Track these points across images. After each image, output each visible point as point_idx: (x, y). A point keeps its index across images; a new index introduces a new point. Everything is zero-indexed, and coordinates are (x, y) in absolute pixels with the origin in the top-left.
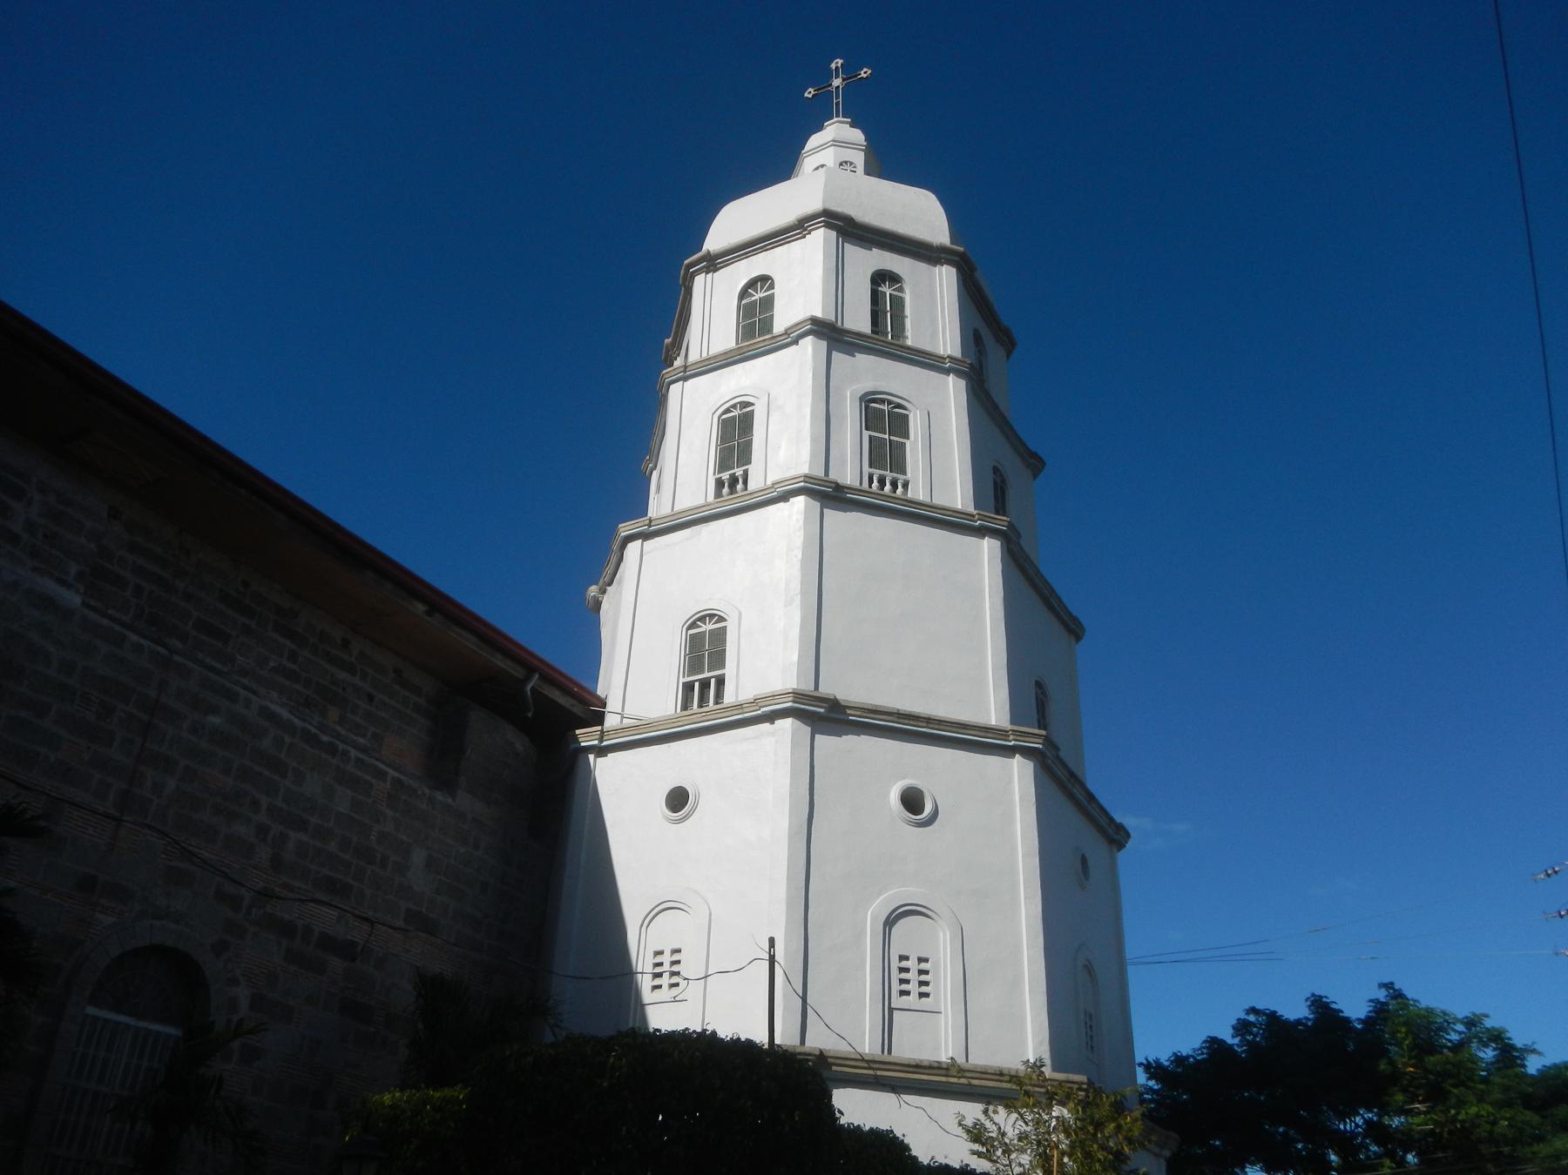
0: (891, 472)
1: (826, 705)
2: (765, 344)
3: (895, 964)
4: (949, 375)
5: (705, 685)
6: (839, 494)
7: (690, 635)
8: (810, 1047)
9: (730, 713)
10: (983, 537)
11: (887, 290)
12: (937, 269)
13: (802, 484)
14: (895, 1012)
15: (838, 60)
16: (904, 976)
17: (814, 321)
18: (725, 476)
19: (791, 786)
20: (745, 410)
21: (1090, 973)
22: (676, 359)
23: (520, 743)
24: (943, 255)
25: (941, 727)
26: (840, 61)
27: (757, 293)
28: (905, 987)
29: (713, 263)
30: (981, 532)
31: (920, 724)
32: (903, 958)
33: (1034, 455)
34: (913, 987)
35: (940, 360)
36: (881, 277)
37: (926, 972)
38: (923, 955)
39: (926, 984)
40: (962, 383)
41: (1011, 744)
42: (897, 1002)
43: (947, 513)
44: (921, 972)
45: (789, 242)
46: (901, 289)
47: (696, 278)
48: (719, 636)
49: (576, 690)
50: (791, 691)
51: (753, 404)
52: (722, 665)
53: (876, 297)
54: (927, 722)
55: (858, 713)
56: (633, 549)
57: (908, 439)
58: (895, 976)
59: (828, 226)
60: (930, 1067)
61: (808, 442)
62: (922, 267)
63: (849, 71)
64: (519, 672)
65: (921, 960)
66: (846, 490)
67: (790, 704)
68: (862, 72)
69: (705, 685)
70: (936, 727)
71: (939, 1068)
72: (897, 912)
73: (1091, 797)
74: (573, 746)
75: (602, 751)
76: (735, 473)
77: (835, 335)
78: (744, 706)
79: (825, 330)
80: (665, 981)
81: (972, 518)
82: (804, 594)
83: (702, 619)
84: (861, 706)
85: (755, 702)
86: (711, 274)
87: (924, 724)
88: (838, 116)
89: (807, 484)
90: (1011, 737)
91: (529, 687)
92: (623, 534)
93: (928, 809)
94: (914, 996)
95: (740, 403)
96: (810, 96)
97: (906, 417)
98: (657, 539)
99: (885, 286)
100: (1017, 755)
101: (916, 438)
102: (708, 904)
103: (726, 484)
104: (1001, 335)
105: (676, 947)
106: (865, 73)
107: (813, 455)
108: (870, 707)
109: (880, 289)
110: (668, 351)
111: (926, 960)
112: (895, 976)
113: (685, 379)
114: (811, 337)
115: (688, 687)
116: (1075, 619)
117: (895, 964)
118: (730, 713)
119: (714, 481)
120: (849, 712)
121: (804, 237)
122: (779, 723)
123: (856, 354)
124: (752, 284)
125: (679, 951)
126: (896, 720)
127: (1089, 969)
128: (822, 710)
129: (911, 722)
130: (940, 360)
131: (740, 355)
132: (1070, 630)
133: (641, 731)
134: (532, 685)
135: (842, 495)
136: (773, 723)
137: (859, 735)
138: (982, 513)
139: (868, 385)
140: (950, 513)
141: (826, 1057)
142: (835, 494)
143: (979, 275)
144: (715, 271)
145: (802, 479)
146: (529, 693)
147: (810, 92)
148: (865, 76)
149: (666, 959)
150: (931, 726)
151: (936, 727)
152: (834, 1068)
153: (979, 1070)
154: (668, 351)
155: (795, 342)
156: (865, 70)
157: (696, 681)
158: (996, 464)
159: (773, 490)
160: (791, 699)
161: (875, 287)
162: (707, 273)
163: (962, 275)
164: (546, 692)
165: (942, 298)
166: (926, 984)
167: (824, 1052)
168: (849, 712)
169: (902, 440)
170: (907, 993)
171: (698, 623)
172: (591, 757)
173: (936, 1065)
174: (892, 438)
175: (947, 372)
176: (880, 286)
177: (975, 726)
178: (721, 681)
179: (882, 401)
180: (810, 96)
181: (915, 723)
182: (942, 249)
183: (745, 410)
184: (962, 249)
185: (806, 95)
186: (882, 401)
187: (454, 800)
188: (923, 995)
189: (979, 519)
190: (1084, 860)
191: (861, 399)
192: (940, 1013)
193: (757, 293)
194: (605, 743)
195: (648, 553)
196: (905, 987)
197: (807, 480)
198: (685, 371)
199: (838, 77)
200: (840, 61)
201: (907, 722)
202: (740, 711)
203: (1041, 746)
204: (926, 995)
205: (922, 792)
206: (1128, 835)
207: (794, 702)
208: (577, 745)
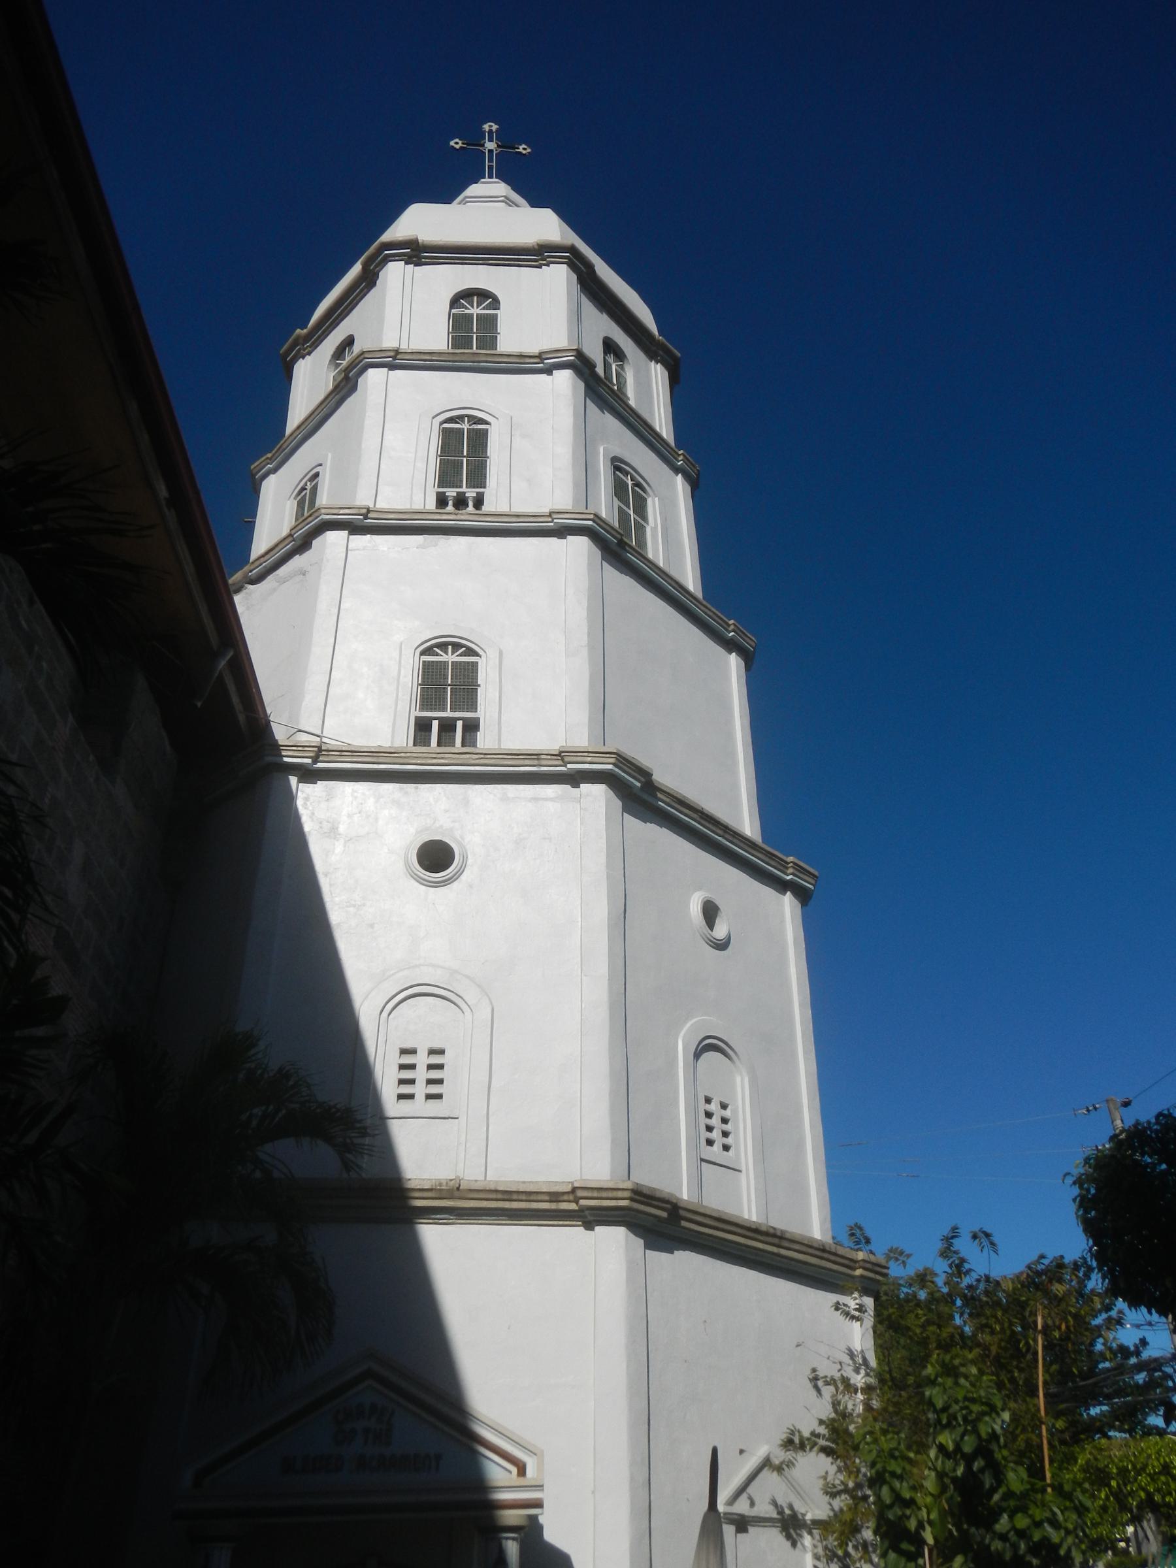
1: (643, 780)
5: (447, 727)
7: (424, 662)
8: (669, 1193)
9: (521, 762)
13: (590, 523)
18: (451, 492)
20: (475, 426)
22: (303, 358)
24: (661, 352)
25: (735, 841)
26: (495, 127)
27: (477, 308)
34: (716, 1135)
41: (788, 878)
47: (390, 264)
49: (254, 690)
51: (487, 423)
54: (725, 832)
55: (668, 800)
57: (648, 524)
59: (572, 265)
60: (767, 1234)
63: (507, 141)
67: (610, 767)
68: (521, 147)
69: (447, 727)
70: (731, 839)
71: (774, 1236)
72: (701, 1046)
76: (445, 493)
78: (543, 757)
79: (586, 371)
81: (726, 626)
82: (591, 647)
83: (443, 646)
84: (671, 792)
85: (561, 755)
88: (491, 177)
89: (595, 525)
90: (790, 870)
93: (720, 931)
94: (717, 1147)
95: (468, 416)
96: (457, 147)
100: (789, 893)
103: (451, 503)
105: (437, 1045)
106: (524, 149)
107: (576, 501)
108: (678, 796)
110: (295, 343)
113: (392, 367)
115: (422, 727)
118: (521, 762)
119: (435, 494)
120: (659, 795)
121: (540, 267)
122: (585, 787)
125: (441, 1052)
126: (698, 819)
128: (639, 785)
133: (381, 760)
137: (661, 827)
138: (737, 624)
139: (618, 452)
144: (417, 265)
145: (592, 517)
147: (457, 143)
149: (422, 1059)
150: (727, 836)
151: (731, 839)
152: (684, 1223)
153: (806, 1242)
154: (295, 343)
155: (548, 371)
157: (435, 718)
159: (550, 520)
160: (612, 760)
162: (407, 263)
168: (659, 795)
172: (293, 780)
173: (772, 1231)
178: (472, 727)
179: (626, 473)
181: (714, 828)
183: (475, 426)
184: (679, 355)
185: (452, 143)
193: (473, 307)
194: (320, 765)
195: (354, 550)
198: (394, 358)
199: (492, 141)
200: (495, 127)
201: (707, 824)
202: (536, 762)
208: (276, 759)
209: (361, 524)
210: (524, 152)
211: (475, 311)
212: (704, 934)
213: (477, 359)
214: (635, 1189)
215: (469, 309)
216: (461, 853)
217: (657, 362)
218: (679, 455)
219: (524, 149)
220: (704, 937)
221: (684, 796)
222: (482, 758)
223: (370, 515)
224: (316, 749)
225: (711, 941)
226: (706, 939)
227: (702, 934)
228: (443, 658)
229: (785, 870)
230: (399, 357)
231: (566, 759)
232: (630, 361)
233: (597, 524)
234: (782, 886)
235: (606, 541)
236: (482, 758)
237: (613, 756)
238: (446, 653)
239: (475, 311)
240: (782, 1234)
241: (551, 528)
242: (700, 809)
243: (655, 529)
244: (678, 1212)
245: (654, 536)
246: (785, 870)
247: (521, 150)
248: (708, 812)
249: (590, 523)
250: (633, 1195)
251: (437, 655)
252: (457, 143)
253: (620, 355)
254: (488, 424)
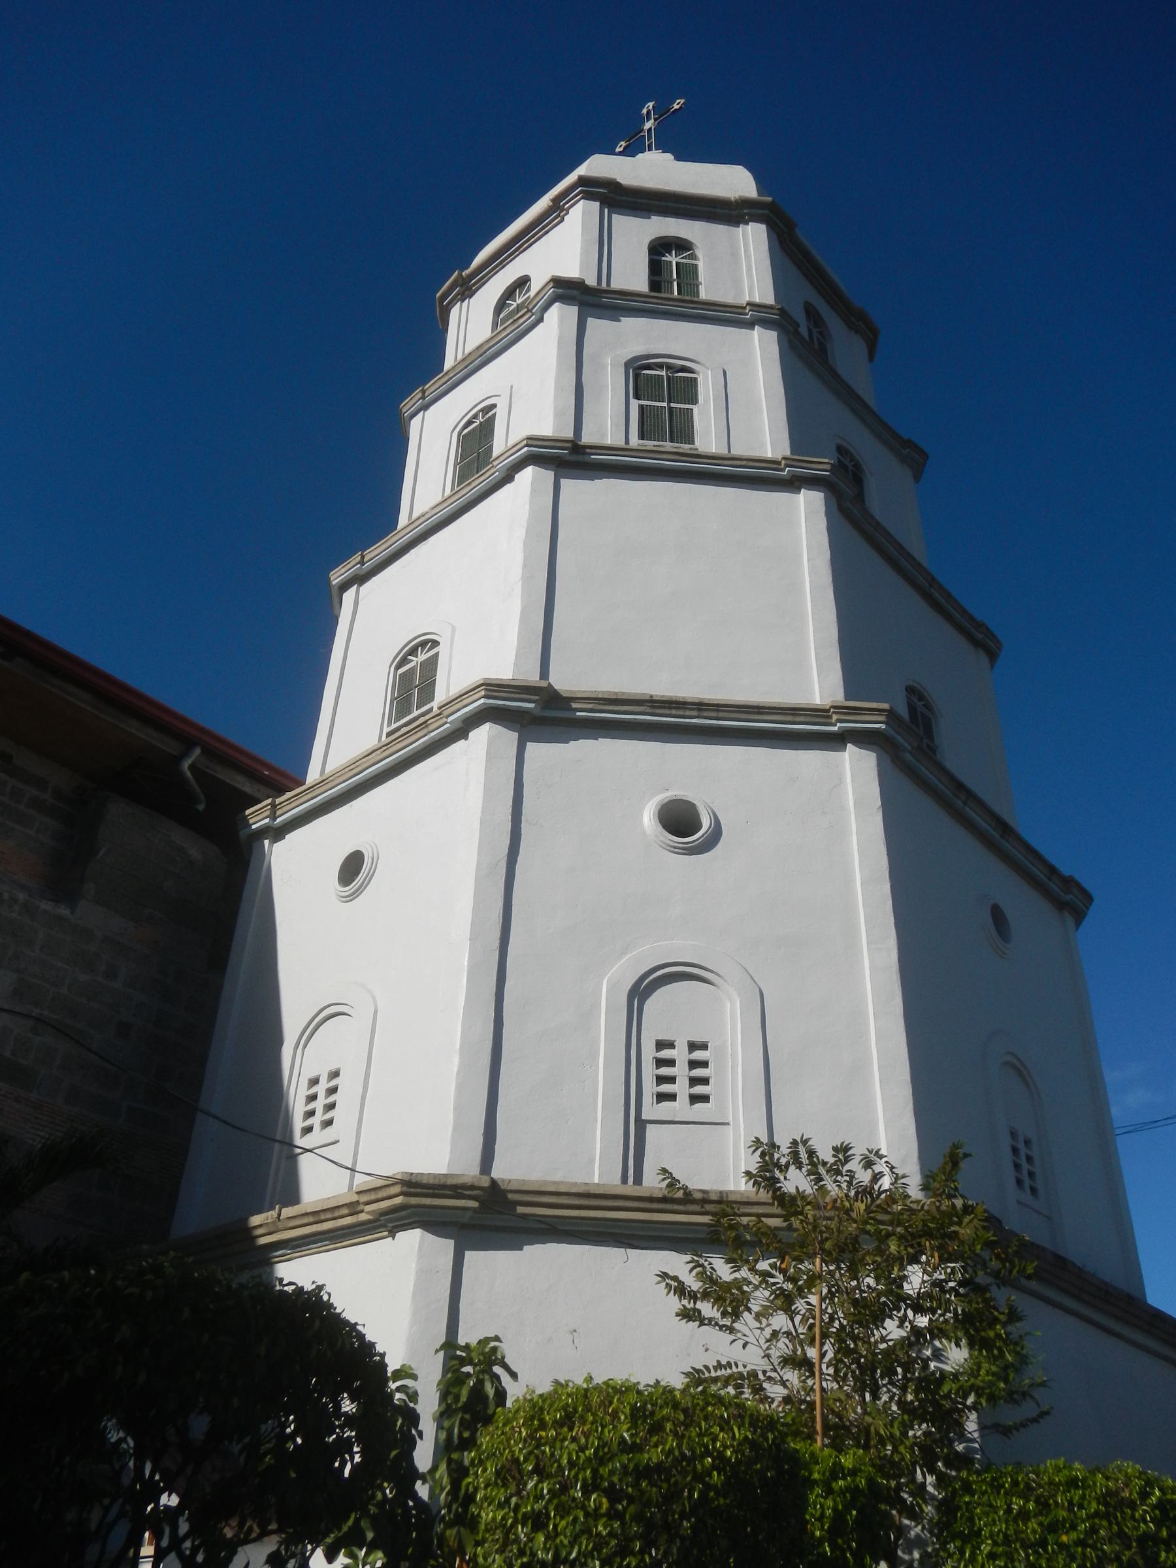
0: (672, 441)
1: (537, 697)
2: (508, 331)
3: (649, 1053)
4: (754, 329)
6: (580, 458)
10: (797, 490)
11: (673, 259)
12: (740, 230)
14: (650, 1128)
15: (649, 104)
16: (665, 1071)
17: (557, 282)
19: (483, 812)
20: (487, 416)
21: (1021, 1075)
23: (195, 848)
25: (721, 714)
26: (651, 104)
28: (666, 1088)
29: (467, 290)
30: (793, 484)
31: (688, 713)
32: (661, 1045)
33: (909, 444)
34: (681, 1088)
35: (740, 310)
36: (659, 248)
37: (704, 1064)
38: (698, 1038)
39: (705, 1081)
40: (772, 336)
41: (836, 728)
42: (651, 1110)
43: (739, 463)
44: (693, 1064)
45: (547, 232)
46: (693, 256)
48: (431, 666)
50: (482, 682)
53: (656, 269)
54: (699, 710)
56: (349, 596)
58: (649, 1071)
59: (589, 196)
61: (552, 418)
62: (720, 229)
63: (661, 111)
64: (171, 747)
65: (693, 1046)
66: (588, 451)
67: (482, 701)
73: (1006, 829)
74: (243, 834)
75: (278, 833)
77: (590, 299)
78: (429, 722)
79: (575, 293)
80: (316, 1121)
82: (527, 579)
83: (413, 652)
86: (467, 301)
87: (694, 713)
90: (835, 717)
91: (186, 764)
92: (334, 583)
95: (482, 410)
97: (696, 379)
98: (374, 579)
99: (671, 255)
100: (849, 745)
101: (707, 400)
102: (373, 997)
104: (853, 319)
105: (334, 1067)
108: (606, 696)
109: (663, 258)
111: (704, 1046)
112: (649, 1071)
113: (425, 407)
114: (557, 304)
116: (980, 625)
117: (649, 1053)
120: (574, 705)
121: (562, 220)
123: (621, 318)
124: (510, 293)
127: (1018, 1069)
128: (531, 705)
129: (674, 712)
130: (740, 310)
131: (481, 356)
132: (976, 644)
134: (190, 761)
135: (586, 458)
136: (466, 737)
139: (636, 348)
140: (744, 463)
141: (504, 1192)
142: (574, 458)
143: (800, 234)
144: (471, 296)
145: (525, 442)
146: (189, 774)
147: (621, 146)
148: (678, 106)
149: (321, 1089)
150: (705, 714)
152: (520, 1210)
155: (540, 320)
156: (678, 101)
158: (844, 444)
160: (483, 693)
161: (655, 257)
162: (463, 301)
163: (779, 236)
164: (219, 776)
165: (748, 257)
166: (705, 1081)
167: (501, 1184)
168: (574, 705)
169: (687, 406)
170: (672, 1097)
171: (410, 657)
172: (266, 842)
174: (673, 405)
175: (750, 325)
176: (664, 256)
177: (774, 708)
179: (660, 366)
180: (621, 149)
181: (681, 712)
182: (745, 203)
183: (487, 416)
184: (770, 199)
186: (660, 366)
187: (72, 913)
188: (695, 1099)
189: (787, 466)
190: (997, 915)
191: (628, 365)
192: (729, 1124)
196: (666, 1088)
197: (530, 442)
198: (423, 398)
200: (651, 104)
201: (667, 712)
202: (425, 731)
203: (883, 726)
204: (705, 1098)
205: (693, 806)
206: (1088, 898)
207: (485, 697)
209: (362, 572)
212: (662, 842)
213: (481, 352)
214: (407, 1178)
216: (371, 855)
217: (747, 224)
218: (750, 311)
220: (664, 845)
221: (616, 693)
222: (384, 751)
223: (365, 560)
224: (269, 807)
225: (675, 848)
226: (670, 848)
227: (660, 843)
229: (829, 721)
230: (426, 394)
232: (698, 245)
233: (535, 446)
234: (837, 741)
235: (559, 457)
236: (384, 751)
237: (483, 687)
238: (417, 657)
240: (721, 1197)
241: (499, 478)
242: (648, 698)
244: (507, 1197)
246: (829, 721)
247: (676, 107)
248: (663, 696)
249: (526, 449)
250: (405, 1189)
251: (411, 661)
252: (621, 146)
253: (682, 246)
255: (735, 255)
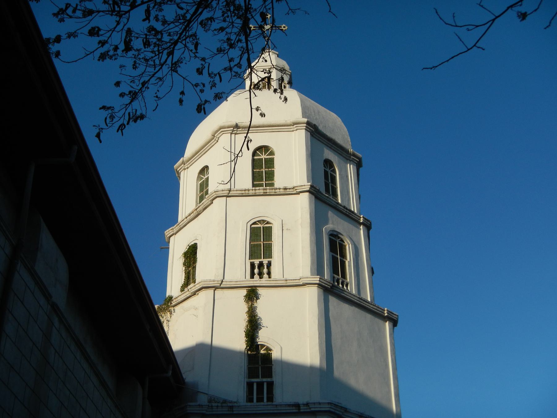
5: (260, 385)
18: (257, 262)
27: (265, 155)
52: (270, 376)
57: (346, 259)
68: (282, 26)
101: (350, 260)
106: (284, 27)
157: (255, 382)
162: (231, 134)
178: (271, 385)
193: (263, 155)
197: (321, 280)
210: (284, 29)
211: (263, 157)
215: (261, 156)
219: (284, 27)
228: (259, 225)
231: (310, 406)
239: (263, 157)
243: (350, 262)
245: (350, 266)
254: (271, 224)
255: (347, 176)
